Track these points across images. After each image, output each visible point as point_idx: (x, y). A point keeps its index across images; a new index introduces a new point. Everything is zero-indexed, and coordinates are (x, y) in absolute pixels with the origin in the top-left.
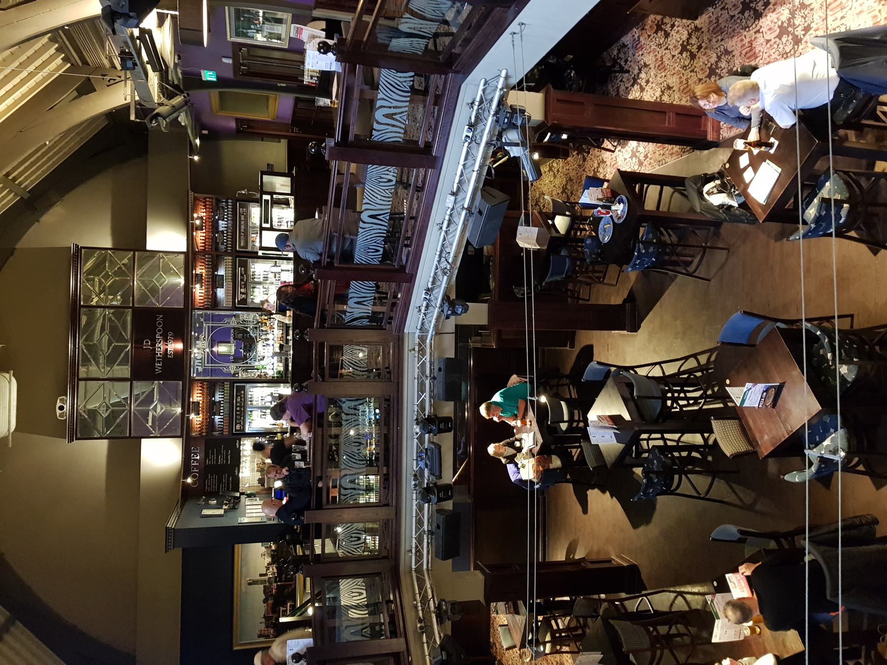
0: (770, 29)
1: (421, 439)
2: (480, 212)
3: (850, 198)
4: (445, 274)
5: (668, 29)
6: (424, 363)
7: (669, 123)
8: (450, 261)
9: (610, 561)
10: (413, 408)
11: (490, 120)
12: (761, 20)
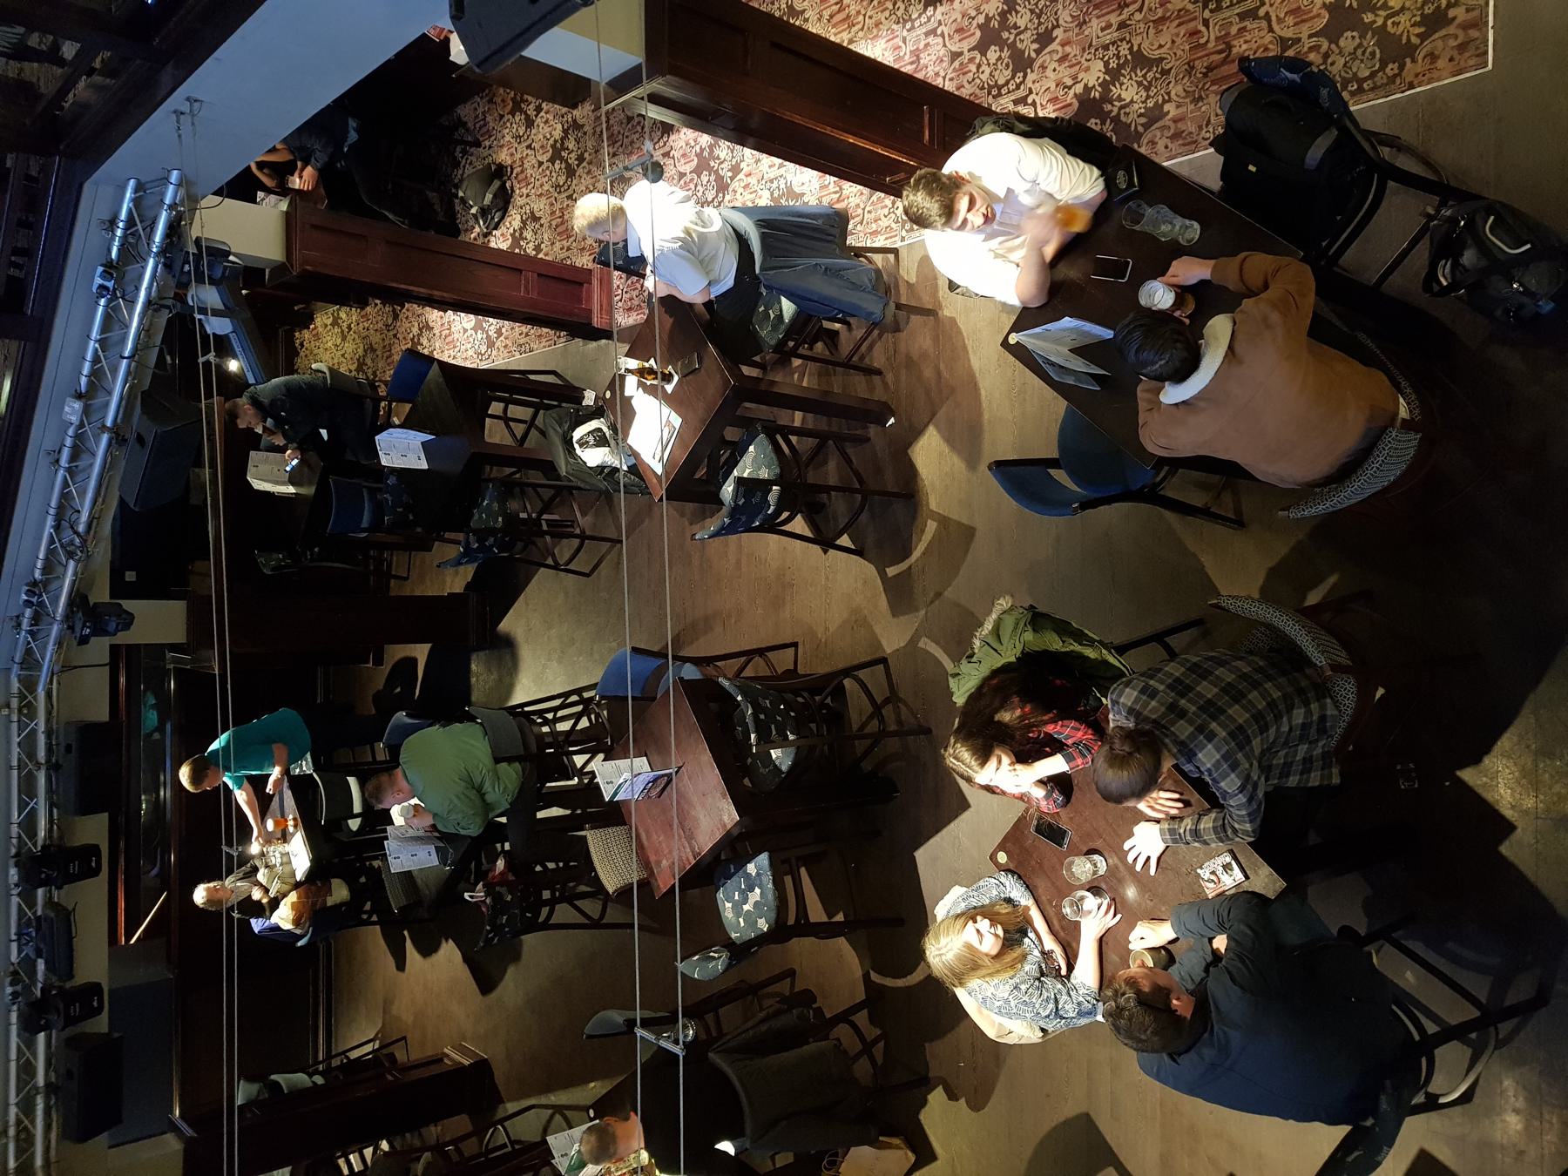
0: (684, 155)
1: (28, 898)
2: (140, 439)
3: (781, 475)
4: (70, 555)
5: (531, 113)
6: (34, 732)
7: (525, 291)
8: (81, 528)
9: (439, 1060)
10: (8, 830)
11: (151, 262)
12: (672, 137)
